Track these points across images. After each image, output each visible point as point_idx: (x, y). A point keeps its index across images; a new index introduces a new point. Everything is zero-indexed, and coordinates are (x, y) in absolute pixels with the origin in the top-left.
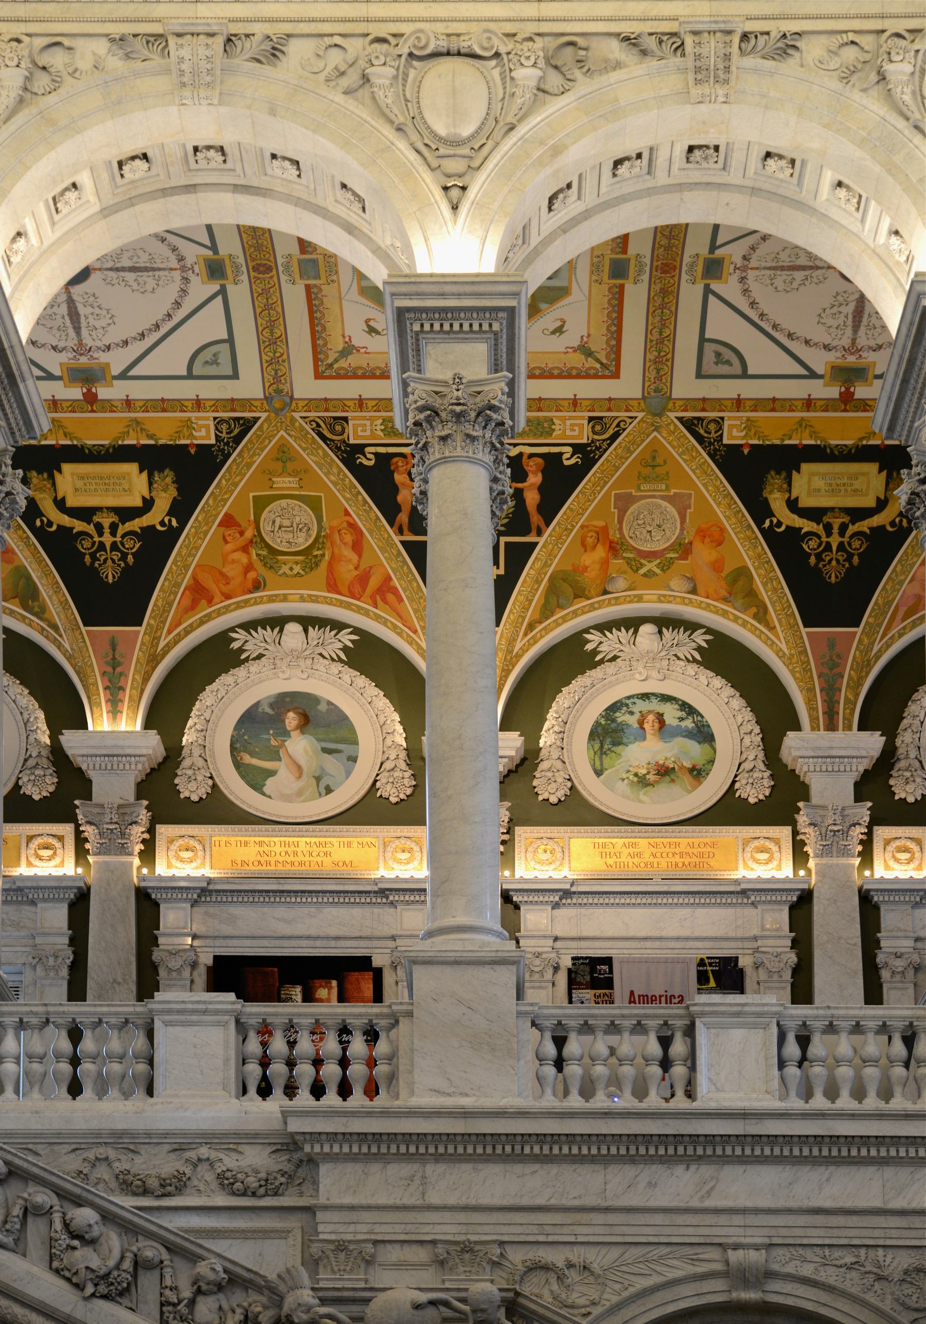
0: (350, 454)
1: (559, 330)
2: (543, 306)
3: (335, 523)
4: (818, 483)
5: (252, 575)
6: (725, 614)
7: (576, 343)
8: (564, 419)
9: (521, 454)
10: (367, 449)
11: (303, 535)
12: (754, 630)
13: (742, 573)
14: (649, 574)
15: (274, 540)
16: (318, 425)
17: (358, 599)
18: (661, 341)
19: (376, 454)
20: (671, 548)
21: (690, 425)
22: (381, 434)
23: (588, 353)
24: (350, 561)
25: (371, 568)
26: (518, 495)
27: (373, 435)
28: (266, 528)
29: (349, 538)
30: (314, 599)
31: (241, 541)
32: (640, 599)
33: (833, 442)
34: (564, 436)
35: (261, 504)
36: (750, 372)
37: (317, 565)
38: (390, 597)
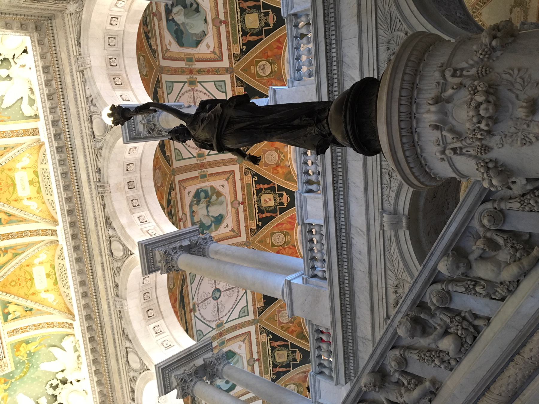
0: (259, 227)
1: (223, 186)
2: (216, 190)
5: (291, 247)
7: (226, 181)
8: (246, 181)
14: (284, 156)
18: (223, 163)
23: (228, 178)
26: (266, 189)
27: (254, 223)
28: (279, 244)
29: (280, 226)
30: (296, 233)
31: (283, 249)
32: (290, 158)
34: (250, 181)
35: (273, 245)
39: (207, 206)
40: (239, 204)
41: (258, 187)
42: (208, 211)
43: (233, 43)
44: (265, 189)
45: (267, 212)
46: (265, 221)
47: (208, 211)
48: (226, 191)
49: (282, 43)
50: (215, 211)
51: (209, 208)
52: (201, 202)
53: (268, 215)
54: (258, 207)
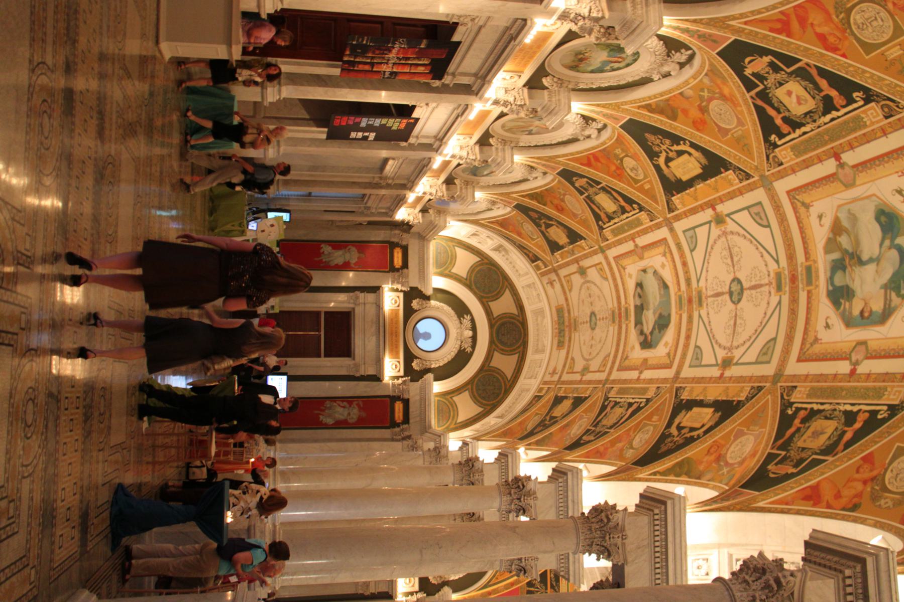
0: (869, 97)
1: (820, 217)
2: (831, 236)
3: (846, 43)
4: (690, 165)
6: (661, 95)
8: (792, 159)
9: (794, 132)
10: (861, 103)
11: (860, 21)
12: (644, 99)
13: (674, 118)
14: (702, 90)
15: (873, 8)
16: (898, 107)
17: (795, 7)
19: (856, 102)
20: (707, 106)
21: (748, 176)
22: (863, 116)
24: (819, 26)
25: (804, 32)
29: (831, 39)
32: (694, 77)
33: (701, 185)
34: (785, 149)
36: (746, 212)
37: (835, 8)
38: (778, 26)
39: (861, 263)
40: (841, 165)
41: (785, 129)
42: (871, 260)
43: (642, 224)
44: (779, 112)
45: (818, 89)
46: (847, 88)
47: (871, 260)
48: (825, 207)
49: (588, 157)
50: (870, 238)
51: (865, 257)
52: (851, 286)
53: (823, 83)
54: (824, 114)
